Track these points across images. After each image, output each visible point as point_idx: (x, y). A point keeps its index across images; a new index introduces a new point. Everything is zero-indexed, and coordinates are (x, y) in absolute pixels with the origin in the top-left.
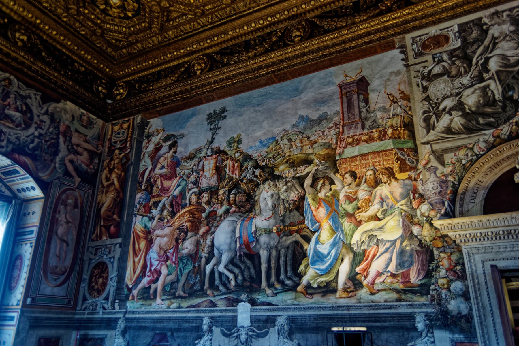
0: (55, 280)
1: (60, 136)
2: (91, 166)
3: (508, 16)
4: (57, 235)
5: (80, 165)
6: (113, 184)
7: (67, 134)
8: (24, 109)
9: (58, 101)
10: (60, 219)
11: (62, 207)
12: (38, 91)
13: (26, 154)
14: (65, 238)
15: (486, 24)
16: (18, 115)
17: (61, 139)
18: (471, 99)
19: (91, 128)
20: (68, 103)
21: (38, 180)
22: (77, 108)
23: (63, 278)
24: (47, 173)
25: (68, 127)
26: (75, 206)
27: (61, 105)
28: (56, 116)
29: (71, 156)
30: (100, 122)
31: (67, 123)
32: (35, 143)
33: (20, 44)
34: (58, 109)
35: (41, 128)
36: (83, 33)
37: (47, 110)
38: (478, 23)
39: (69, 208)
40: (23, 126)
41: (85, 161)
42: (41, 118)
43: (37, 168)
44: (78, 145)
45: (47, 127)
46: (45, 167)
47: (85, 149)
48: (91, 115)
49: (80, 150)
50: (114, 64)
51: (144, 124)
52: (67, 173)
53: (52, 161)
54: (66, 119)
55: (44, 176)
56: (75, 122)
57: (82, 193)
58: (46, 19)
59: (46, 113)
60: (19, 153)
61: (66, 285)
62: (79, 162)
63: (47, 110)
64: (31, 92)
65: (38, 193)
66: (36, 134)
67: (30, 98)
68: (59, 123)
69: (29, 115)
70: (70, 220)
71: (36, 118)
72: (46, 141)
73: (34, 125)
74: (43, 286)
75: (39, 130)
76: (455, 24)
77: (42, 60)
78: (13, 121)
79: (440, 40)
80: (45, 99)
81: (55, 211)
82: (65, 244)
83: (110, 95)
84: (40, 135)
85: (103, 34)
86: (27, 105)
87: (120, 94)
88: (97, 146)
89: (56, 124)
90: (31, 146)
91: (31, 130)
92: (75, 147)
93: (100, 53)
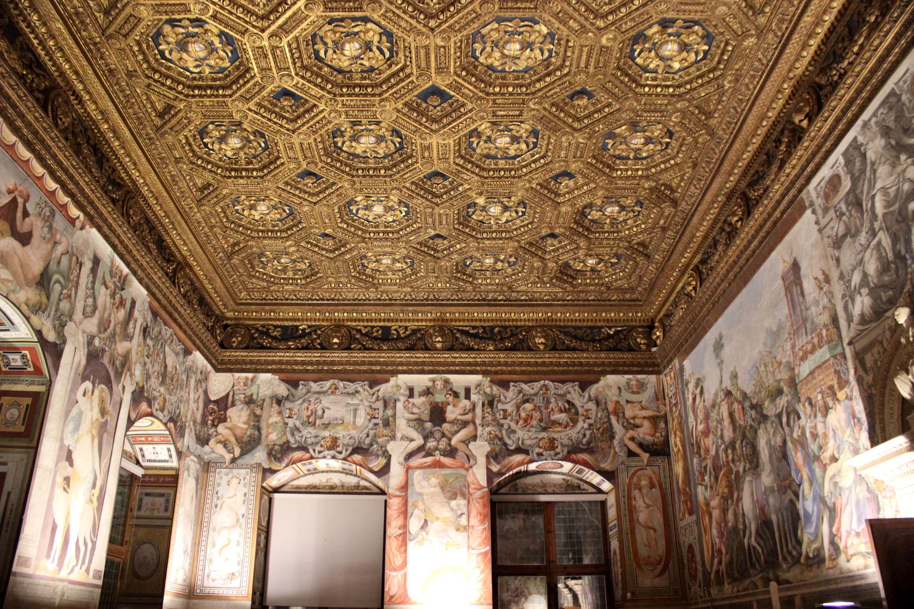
0: (652, 571)
1: (612, 417)
2: (658, 434)
3: (876, 123)
4: (639, 523)
5: (644, 439)
6: (679, 450)
7: (618, 412)
8: (567, 406)
9: (597, 381)
10: (637, 505)
11: (636, 493)
12: (573, 381)
13: (582, 451)
14: (650, 525)
15: (862, 144)
16: (563, 415)
17: (613, 419)
18: (872, 267)
19: (644, 391)
20: (609, 376)
21: (602, 472)
22: (620, 376)
23: (660, 567)
24: (609, 461)
25: (618, 402)
26: (652, 486)
27: (602, 383)
28: (600, 397)
29: (631, 433)
30: (653, 378)
31: (615, 398)
32: (588, 436)
33: (542, 347)
34: (601, 389)
35: (589, 418)
36: (592, 298)
37: (590, 396)
38: (855, 145)
39: (644, 491)
40: (571, 424)
41: (648, 431)
42: (586, 407)
43: (597, 461)
44: (634, 418)
45: (594, 413)
46: (605, 456)
47: (644, 418)
48: (639, 376)
49: (638, 421)
50: (641, 305)
51: (682, 369)
52: (631, 454)
53: (610, 447)
54: (612, 396)
55: (606, 466)
56: (624, 393)
57: (656, 468)
58: (554, 309)
59: (590, 399)
60: (575, 453)
61: (666, 575)
62: (641, 436)
63: (590, 396)
64: (569, 386)
65: (606, 486)
66: (586, 426)
67: (569, 393)
68: (606, 403)
69: (573, 411)
70: (651, 503)
71: (581, 410)
72: (598, 429)
73: (581, 419)
74: (640, 580)
75: (588, 421)
76: (837, 155)
77: (568, 349)
78: (560, 424)
79: (834, 182)
80: (584, 386)
81: (629, 498)
82: (651, 531)
83: (652, 343)
84: (590, 425)
85: (608, 288)
86: (568, 402)
87: (658, 337)
88: (658, 408)
89: (603, 406)
90: (585, 441)
91: (580, 424)
92: (632, 421)
93: (621, 304)
